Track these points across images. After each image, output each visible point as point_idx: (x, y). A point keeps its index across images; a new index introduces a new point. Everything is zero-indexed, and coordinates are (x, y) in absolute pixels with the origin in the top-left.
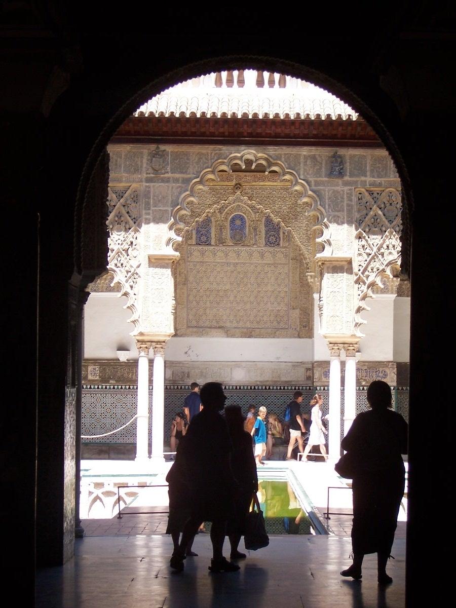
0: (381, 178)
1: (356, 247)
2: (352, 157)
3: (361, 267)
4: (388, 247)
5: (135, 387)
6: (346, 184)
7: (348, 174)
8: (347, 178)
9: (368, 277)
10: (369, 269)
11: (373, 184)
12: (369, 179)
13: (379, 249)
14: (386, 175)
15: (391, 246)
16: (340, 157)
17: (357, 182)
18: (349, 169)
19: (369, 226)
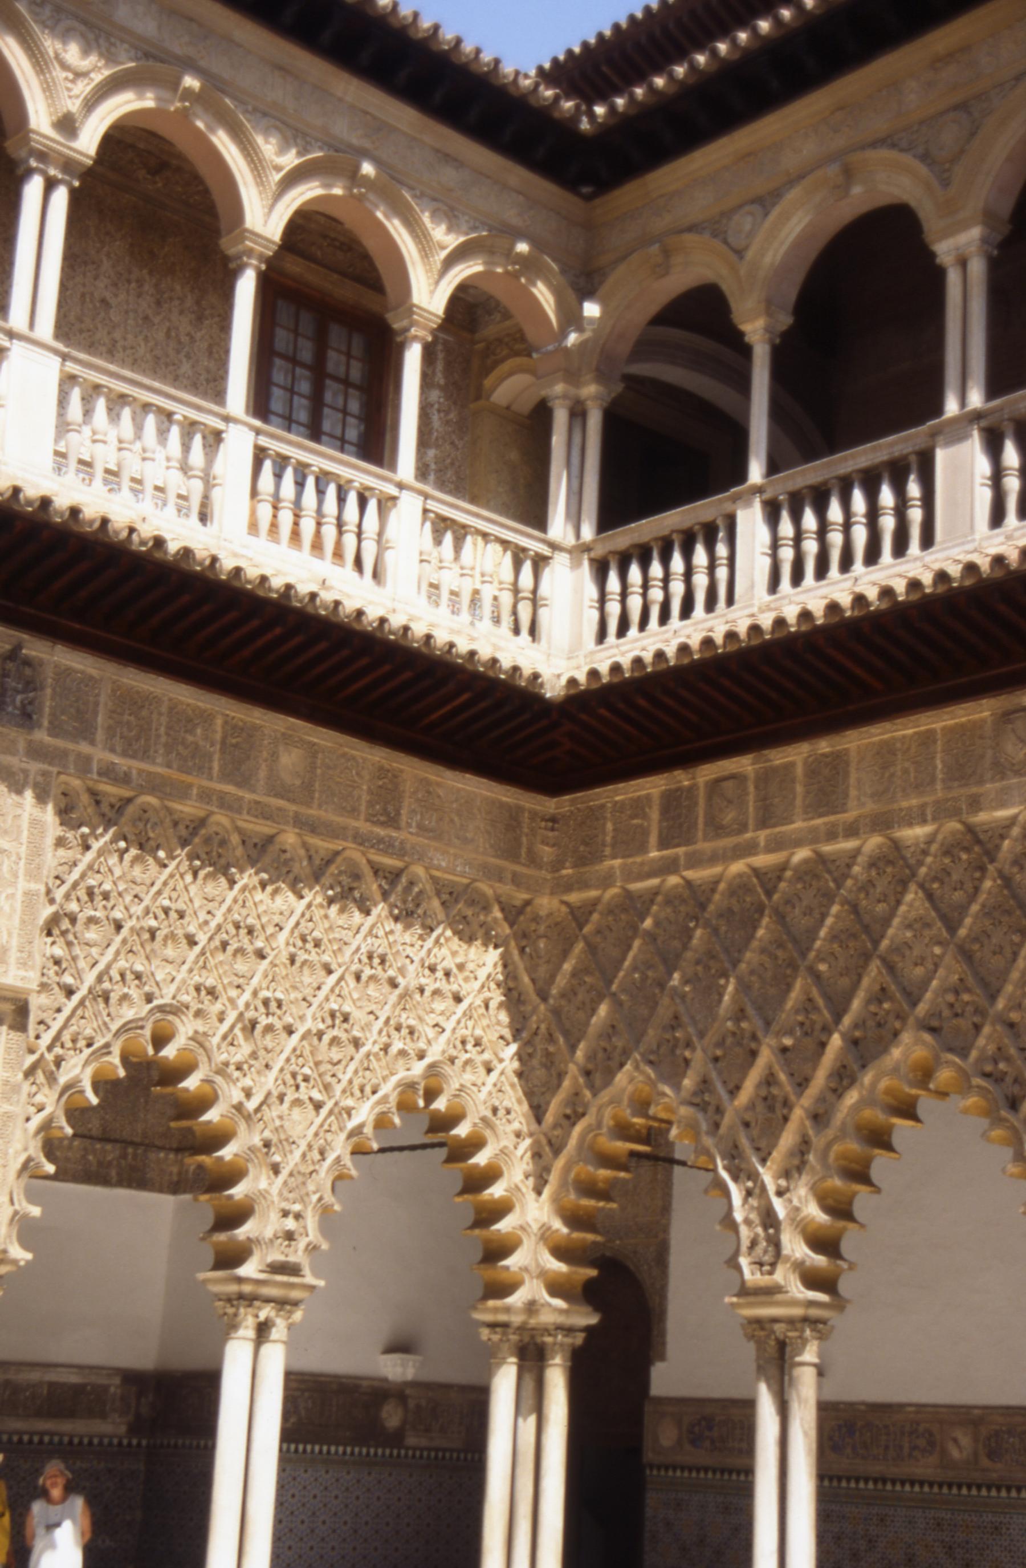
0: (133, 757)
1: (39, 960)
2: (64, 673)
3: (42, 1027)
4: (122, 975)
5: (477, 1457)
6: (36, 752)
7: (46, 723)
8: (41, 736)
9: (58, 1062)
10: (66, 1037)
11: (108, 772)
12: (100, 755)
13: (99, 979)
14: (145, 755)
15: (129, 976)
16: (27, 662)
17: (65, 753)
18: (51, 707)
19: (78, 900)
